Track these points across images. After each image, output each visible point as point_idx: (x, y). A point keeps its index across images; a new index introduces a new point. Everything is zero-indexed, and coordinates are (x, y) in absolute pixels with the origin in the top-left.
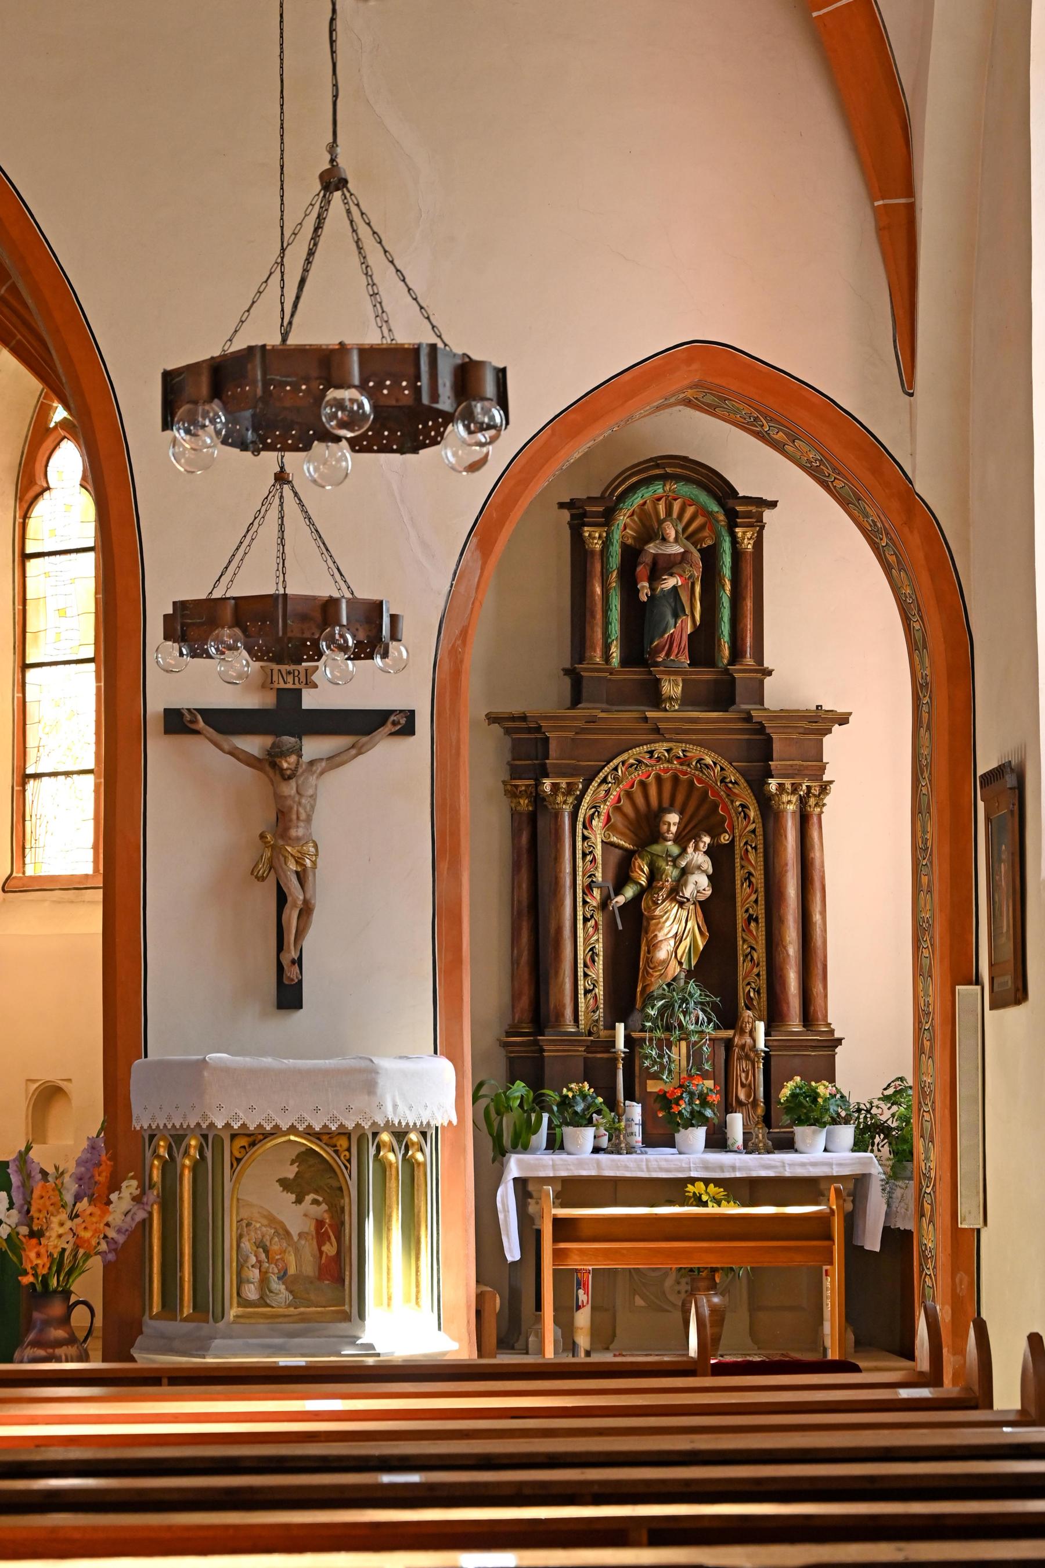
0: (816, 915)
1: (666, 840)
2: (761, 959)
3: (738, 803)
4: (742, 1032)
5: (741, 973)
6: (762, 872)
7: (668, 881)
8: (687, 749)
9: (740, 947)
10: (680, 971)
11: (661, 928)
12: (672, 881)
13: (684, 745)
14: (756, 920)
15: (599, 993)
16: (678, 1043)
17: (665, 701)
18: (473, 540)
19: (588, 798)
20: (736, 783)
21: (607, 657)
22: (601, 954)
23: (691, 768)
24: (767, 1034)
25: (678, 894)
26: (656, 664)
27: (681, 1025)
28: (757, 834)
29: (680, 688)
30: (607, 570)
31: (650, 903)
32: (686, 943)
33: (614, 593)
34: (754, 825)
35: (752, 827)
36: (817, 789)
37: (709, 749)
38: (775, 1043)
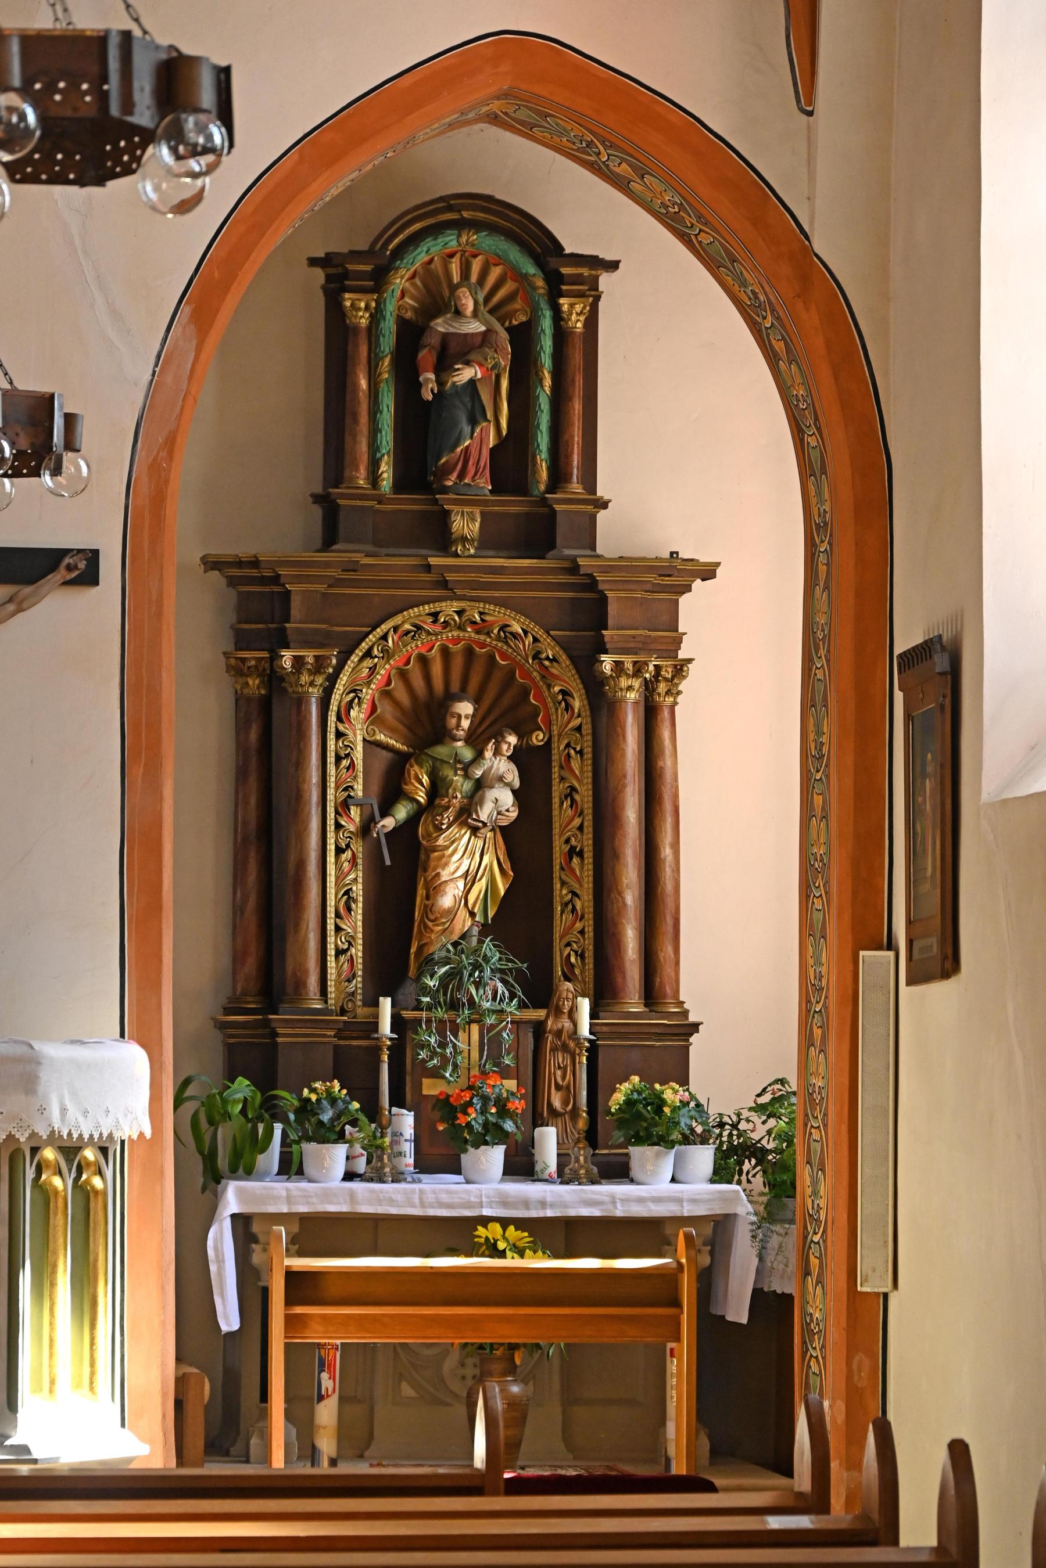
0: (664, 848)
1: (455, 739)
2: (586, 910)
3: (557, 689)
4: (558, 1012)
5: (558, 929)
6: (590, 786)
8: (487, 611)
9: (557, 893)
10: (472, 925)
11: (446, 864)
12: (462, 797)
13: (482, 606)
14: (581, 854)
15: (356, 955)
16: (467, 1026)
17: (455, 542)
18: (186, 310)
19: (345, 678)
20: (554, 660)
21: (374, 479)
22: (361, 899)
23: (490, 637)
24: (593, 1015)
25: (470, 815)
26: (445, 490)
27: (471, 1002)
28: (584, 732)
29: (477, 524)
30: (376, 355)
31: (431, 828)
32: (481, 886)
33: (386, 389)
34: (579, 720)
35: (576, 722)
36: (670, 670)
37: (517, 612)
38: (605, 1029)
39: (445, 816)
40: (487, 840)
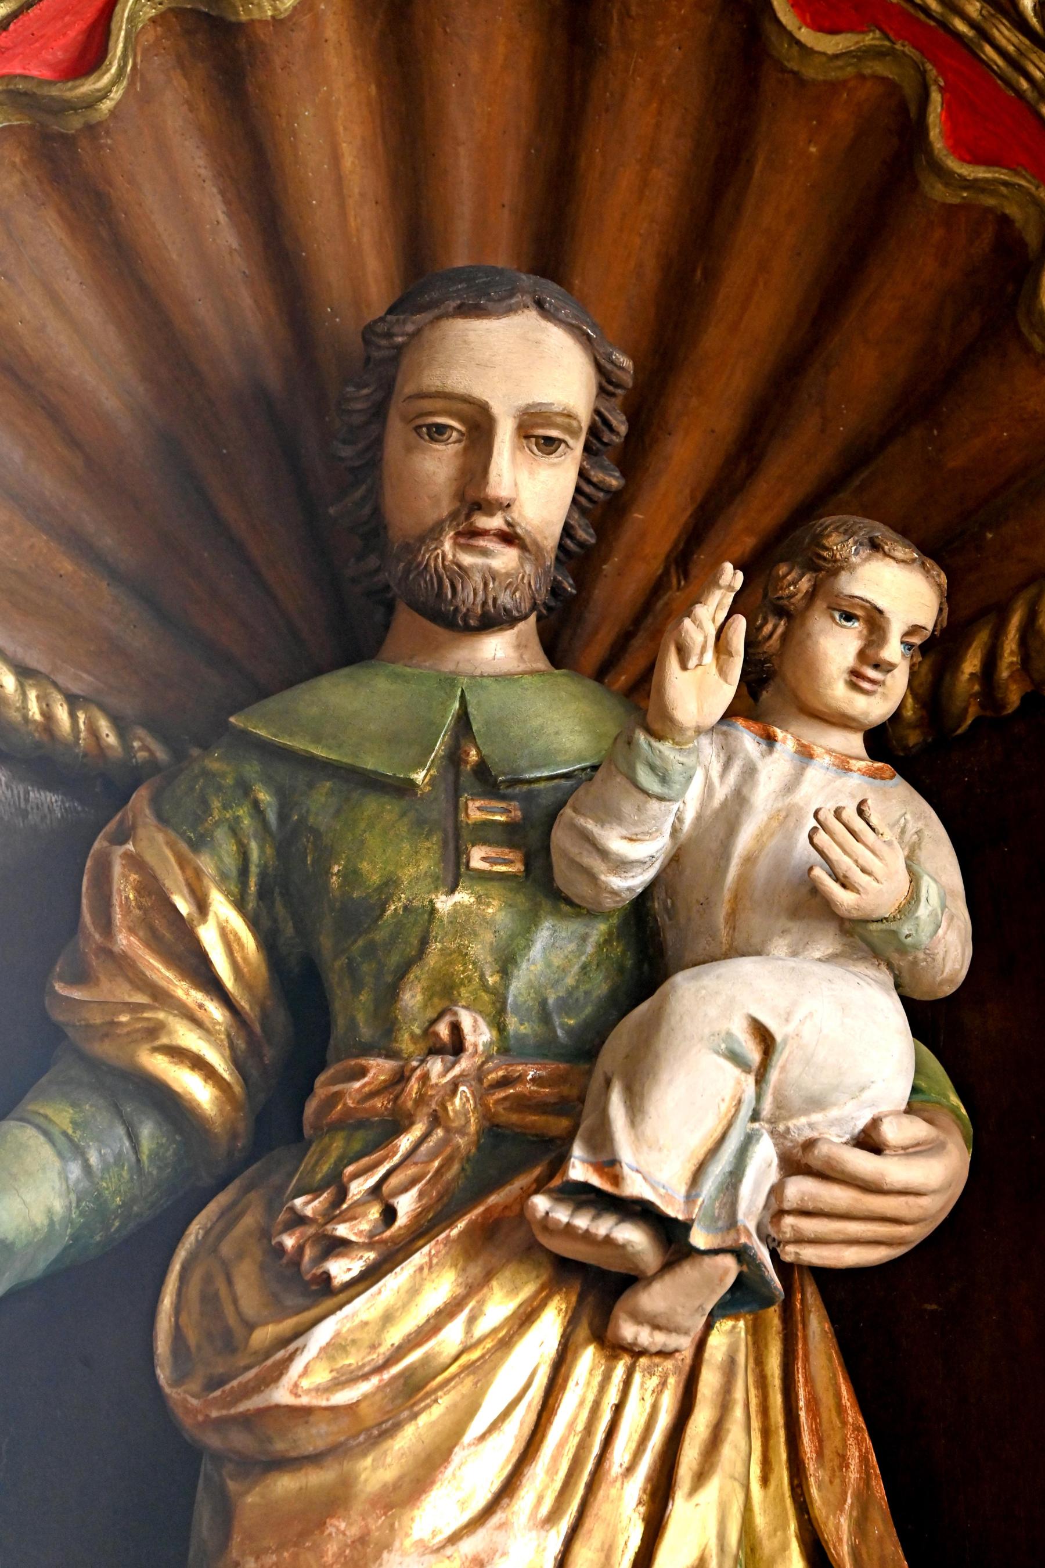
7: (457, 1046)
39: (358, 1188)
40: (709, 1381)
